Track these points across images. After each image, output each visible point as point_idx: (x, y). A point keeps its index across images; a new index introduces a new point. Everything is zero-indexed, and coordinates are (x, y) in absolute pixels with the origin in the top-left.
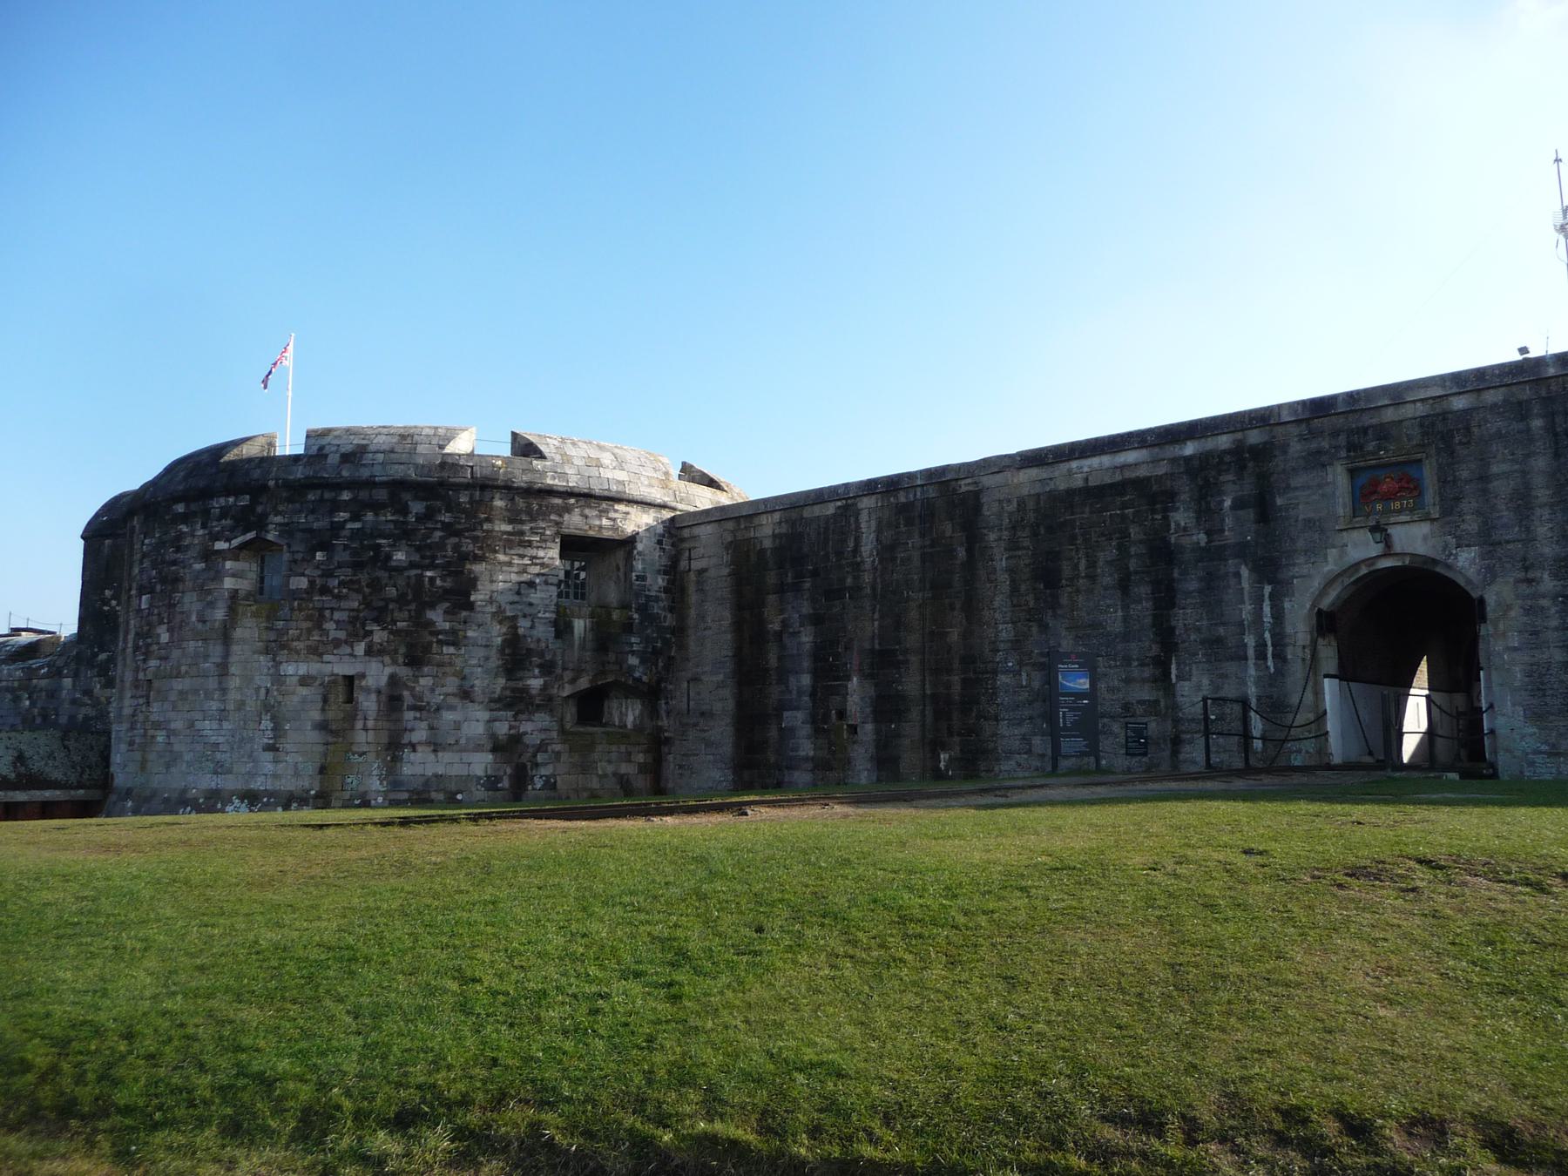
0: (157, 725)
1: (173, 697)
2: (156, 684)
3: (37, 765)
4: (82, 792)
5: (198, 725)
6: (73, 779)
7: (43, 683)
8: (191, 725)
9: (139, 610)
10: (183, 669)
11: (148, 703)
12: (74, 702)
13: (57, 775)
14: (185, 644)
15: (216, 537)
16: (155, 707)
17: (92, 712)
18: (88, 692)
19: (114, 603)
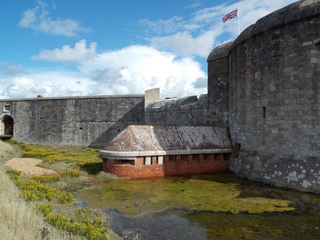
0: (273, 126)
1: (281, 113)
2: (268, 108)
3: (210, 139)
4: (226, 150)
5: (299, 127)
6: (222, 145)
7: (196, 111)
8: (295, 126)
9: (253, 80)
10: (287, 102)
11: (265, 117)
12: (208, 117)
13: (216, 143)
14: (286, 91)
15: (302, 41)
16: (269, 118)
17: (216, 120)
18: (214, 113)
19: (222, 82)
